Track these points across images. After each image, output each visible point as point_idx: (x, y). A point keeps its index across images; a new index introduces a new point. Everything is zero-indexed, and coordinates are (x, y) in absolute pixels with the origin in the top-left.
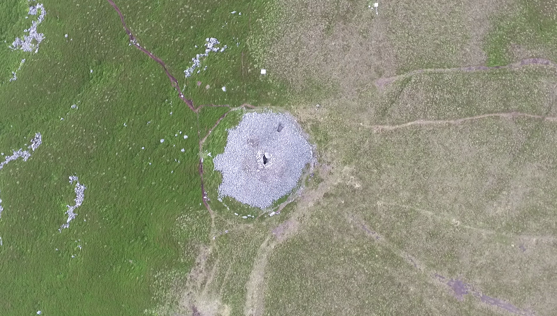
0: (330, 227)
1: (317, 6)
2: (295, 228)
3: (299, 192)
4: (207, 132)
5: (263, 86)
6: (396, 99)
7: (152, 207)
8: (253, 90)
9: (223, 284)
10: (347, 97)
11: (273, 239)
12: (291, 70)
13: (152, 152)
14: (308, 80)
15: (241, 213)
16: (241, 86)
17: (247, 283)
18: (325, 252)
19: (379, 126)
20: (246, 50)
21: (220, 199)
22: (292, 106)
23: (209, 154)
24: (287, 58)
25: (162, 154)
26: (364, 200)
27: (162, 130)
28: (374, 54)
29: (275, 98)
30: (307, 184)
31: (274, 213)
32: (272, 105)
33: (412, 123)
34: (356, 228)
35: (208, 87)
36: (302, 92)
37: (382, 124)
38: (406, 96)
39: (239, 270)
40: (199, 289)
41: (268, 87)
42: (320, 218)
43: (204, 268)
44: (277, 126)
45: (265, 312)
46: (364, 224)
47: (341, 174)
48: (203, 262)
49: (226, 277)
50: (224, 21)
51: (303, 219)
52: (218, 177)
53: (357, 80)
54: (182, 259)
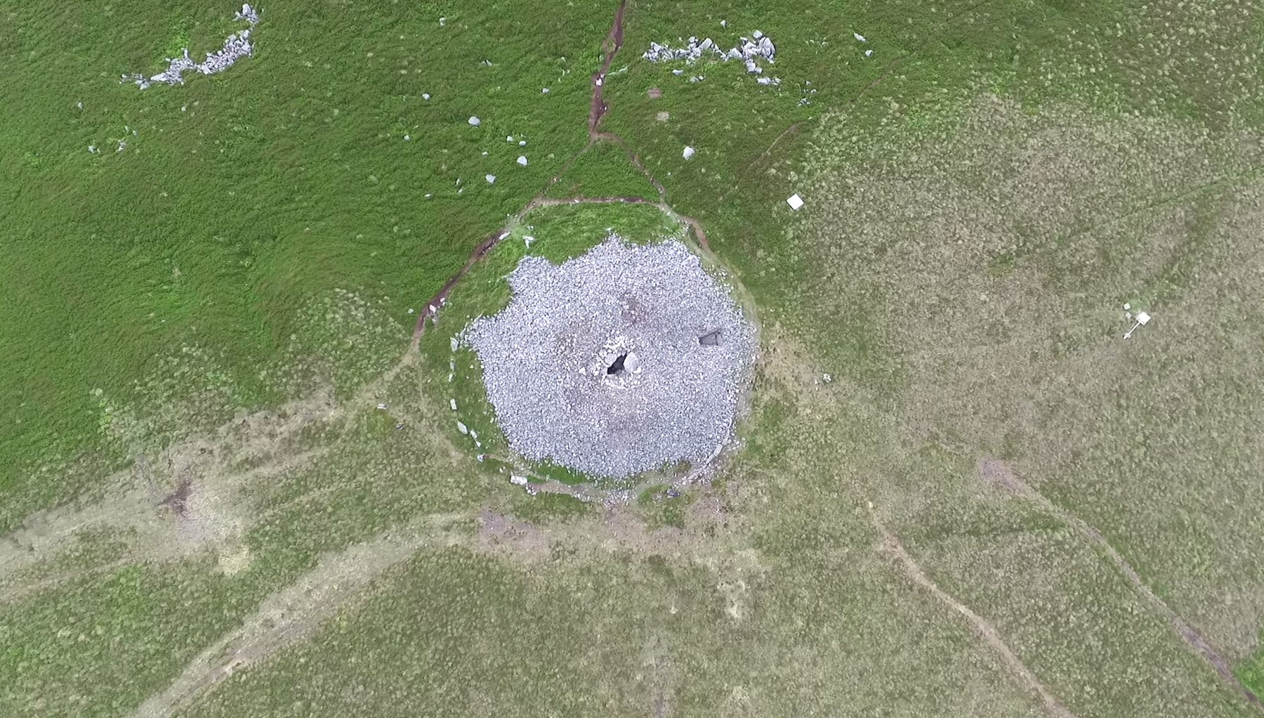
0: (598, 628)
1: (1027, 196)
2: (530, 555)
3: (612, 496)
4: (571, 196)
6: (987, 534)
7: (322, 218)
8: (738, 215)
9: (286, 505)
11: (469, 528)
12: (850, 256)
13: (433, 122)
14: (861, 309)
15: (465, 412)
16: (725, 180)
17: (329, 555)
18: (535, 667)
19: (900, 548)
20: (807, 127)
21: (454, 342)
22: (778, 325)
23: (529, 239)
24: (867, 228)
25: (446, 142)
26: (716, 654)
27: (497, 102)
28: (1039, 404)
29: (763, 273)
30: (645, 499)
31: (523, 481)
32: (744, 281)
33: (970, 614)
34: (643, 690)
35: (663, 116)
36: (827, 318)
37: (908, 549)
38: (1012, 550)
39: (341, 512)
40: (234, 463)
41: (774, 240)
42: (596, 590)
43: (286, 435)
44: (709, 327)
45: (302, 646)
46: (667, 697)
47: (730, 558)
48: (297, 422)
49: (304, 499)
50: (825, 33)
52: (498, 298)
53: (952, 415)
54: (264, 373)
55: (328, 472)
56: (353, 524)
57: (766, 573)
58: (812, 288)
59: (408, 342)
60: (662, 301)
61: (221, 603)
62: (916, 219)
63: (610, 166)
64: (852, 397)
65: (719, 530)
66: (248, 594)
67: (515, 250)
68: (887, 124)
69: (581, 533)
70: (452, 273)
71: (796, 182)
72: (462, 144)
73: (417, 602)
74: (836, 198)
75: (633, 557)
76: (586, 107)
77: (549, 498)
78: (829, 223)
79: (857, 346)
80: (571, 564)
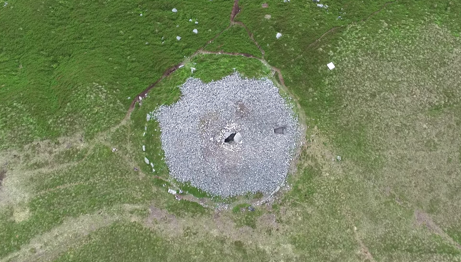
1: (451, 77)
3: (219, 206)
4: (217, 50)
5: (314, 76)
6: (416, 252)
7: (94, 48)
8: (301, 69)
9: (52, 189)
10: (374, 187)
11: (143, 214)
12: (357, 96)
13: (154, 9)
14: (360, 124)
16: (296, 51)
17: (70, 218)
19: (369, 254)
20: (341, 30)
21: (148, 116)
22: (316, 128)
23: (193, 69)
25: (160, 19)
28: (450, 186)
29: (311, 100)
30: (237, 210)
31: (174, 192)
32: (301, 103)
35: (268, 17)
37: (373, 255)
39: (79, 197)
40: (29, 164)
41: (318, 84)
42: (205, 256)
43: (57, 153)
44: (280, 124)
48: (64, 147)
49: (62, 187)
51: (190, 236)
52: (174, 96)
53: (403, 186)
54: (51, 120)
55: (75, 175)
56: (84, 203)
57: (296, 258)
58: (336, 110)
59: (125, 113)
60: (258, 107)
61: (11, 237)
62: (393, 82)
63: (238, 38)
64: (351, 170)
65: (273, 232)
66: (27, 232)
67: (186, 74)
68: (381, 33)
69: (202, 224)
70: (153, 82)
71: (332, 56)
72: (167, 21)
73: (111, 249)
74: (352, 67)
75: (227, 241)
76: (230, 9)
77: (186, 203)
78: (348, 79)
79: (357, 144)
80: (194, 240)
